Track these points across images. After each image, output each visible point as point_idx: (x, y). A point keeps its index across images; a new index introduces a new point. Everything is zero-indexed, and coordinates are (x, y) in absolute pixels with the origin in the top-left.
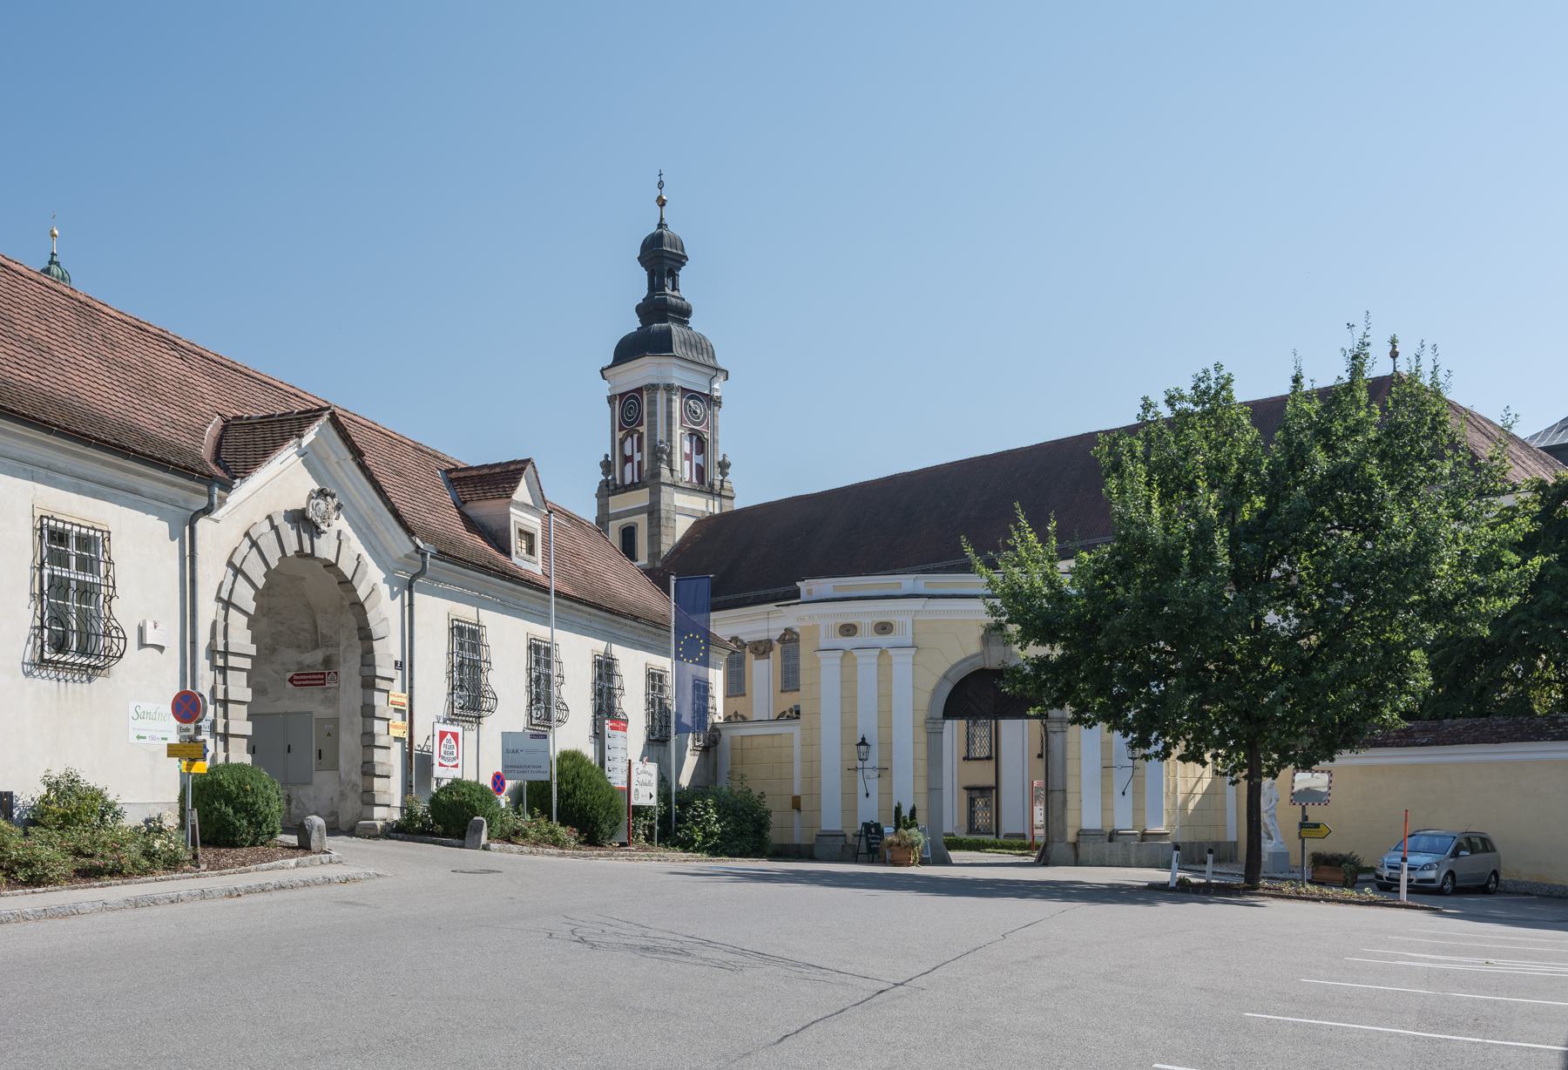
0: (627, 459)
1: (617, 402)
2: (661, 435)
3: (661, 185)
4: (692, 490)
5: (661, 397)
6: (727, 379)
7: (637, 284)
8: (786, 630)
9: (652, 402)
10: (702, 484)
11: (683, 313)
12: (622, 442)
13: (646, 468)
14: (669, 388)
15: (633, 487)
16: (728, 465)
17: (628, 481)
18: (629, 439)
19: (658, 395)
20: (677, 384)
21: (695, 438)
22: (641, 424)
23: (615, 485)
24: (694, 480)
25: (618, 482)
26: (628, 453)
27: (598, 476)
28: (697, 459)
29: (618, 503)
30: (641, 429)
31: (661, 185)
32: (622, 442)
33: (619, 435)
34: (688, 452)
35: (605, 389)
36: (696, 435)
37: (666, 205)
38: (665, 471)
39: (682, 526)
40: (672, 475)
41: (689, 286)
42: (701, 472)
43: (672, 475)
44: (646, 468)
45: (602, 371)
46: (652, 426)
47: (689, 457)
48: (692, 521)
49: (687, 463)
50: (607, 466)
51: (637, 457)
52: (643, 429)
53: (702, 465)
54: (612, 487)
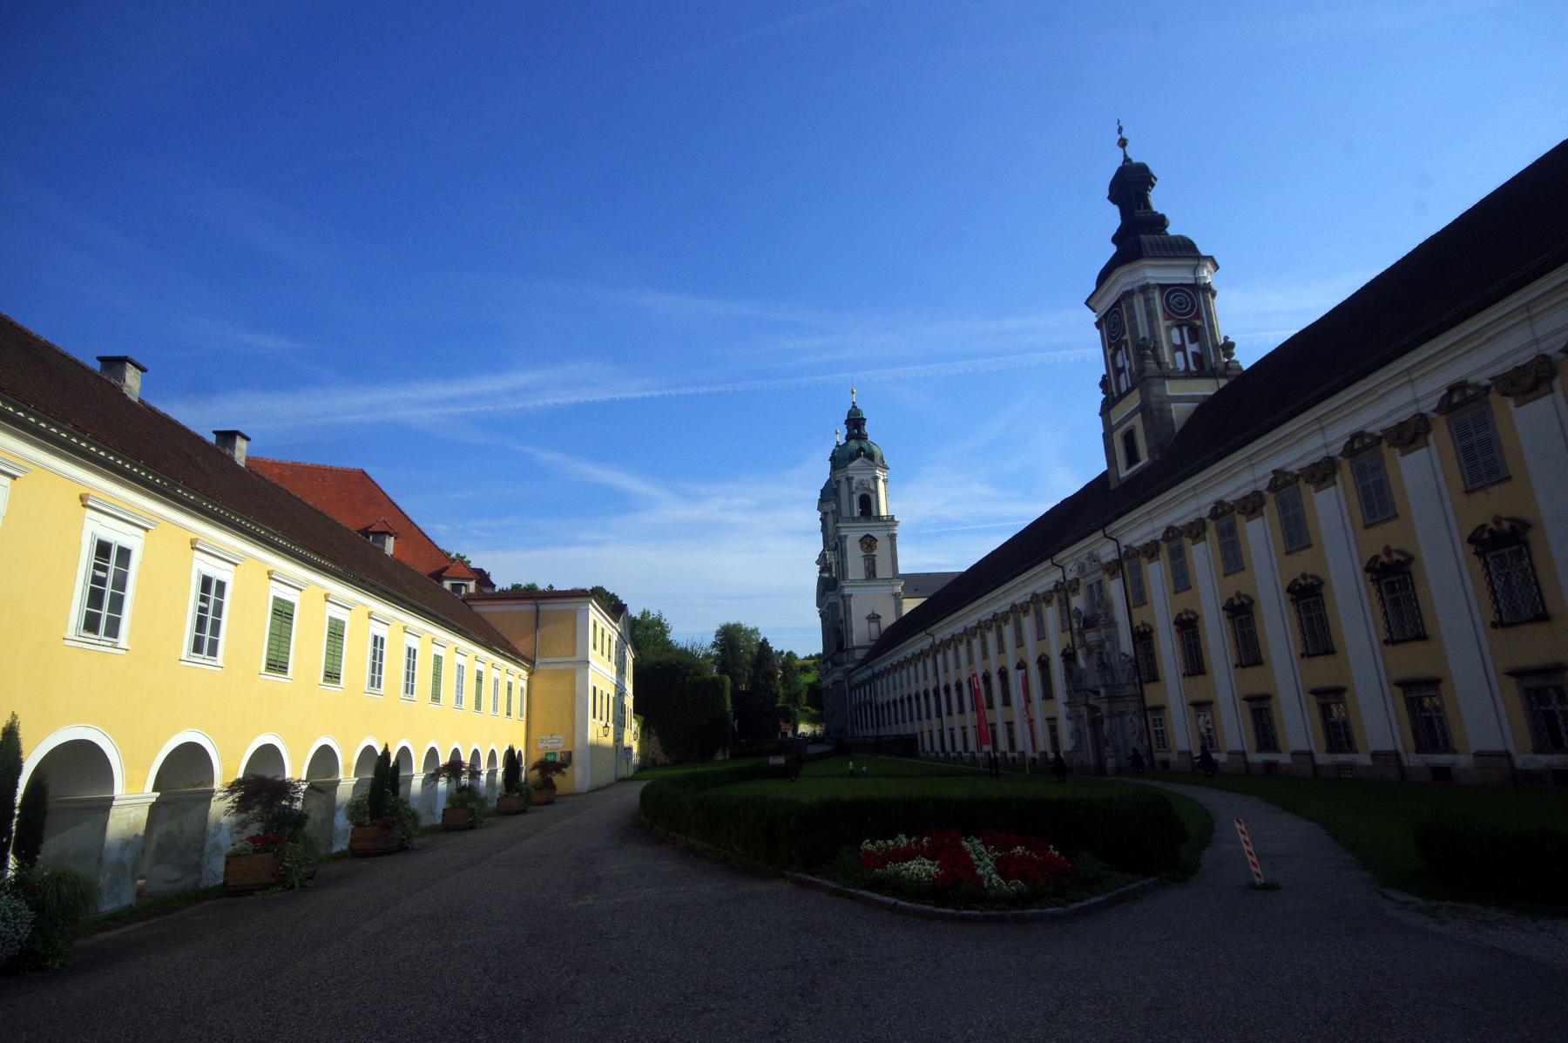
0: (1119, 371)
1: (1104, 325)
2: (1143, 331)
3: (1120, 130)
4: (1188, 375)
5: (1138, 302)
6: (1216, 267)
7: (1112, 218)
8: (1274, 472)
9: (1131, 308)
10: (1202, 368)
11: (1160, 222)
12: (1114, 357)
13: (1134, 370)
14: (1145, 289)
15: (1129, 391)
16: (1232, 345)
17: (1124, 389)
18: (1120, 352)
19: (1135, 300)
20: (1153, 282)
21: (1185, 330)
22: (1124, 333)
23: (1113, 398)
24: (1192, 368)
25: (1115, 395)
26: (1120, 364)
27: (1100, 396)
28: (1192, 348)
29: (1117, 414)
30: (1125, 338)
31: (1120, 130)
32: (1114, 357)
33: (1110, 352)
34: (1177, 341)
35: (1092, 318)
36: (1186, 325)
37: (1129, 144)
38: (1151, 364)
39: (1180, 413)
40: (1160, 368)
41: (1158, 200)
42: (1198, 358)
43: (1160, 368)
44: (1134, 370)
45: (1087, 303)
46: (1134, 328)
47: (1182, 348)
48: (1193, 406)
49: (1179, 355)
50: (1104, 384)
51: (1127, 366)
52: (1127, 337)
53: (1199, 352)
54: (1110, 402)
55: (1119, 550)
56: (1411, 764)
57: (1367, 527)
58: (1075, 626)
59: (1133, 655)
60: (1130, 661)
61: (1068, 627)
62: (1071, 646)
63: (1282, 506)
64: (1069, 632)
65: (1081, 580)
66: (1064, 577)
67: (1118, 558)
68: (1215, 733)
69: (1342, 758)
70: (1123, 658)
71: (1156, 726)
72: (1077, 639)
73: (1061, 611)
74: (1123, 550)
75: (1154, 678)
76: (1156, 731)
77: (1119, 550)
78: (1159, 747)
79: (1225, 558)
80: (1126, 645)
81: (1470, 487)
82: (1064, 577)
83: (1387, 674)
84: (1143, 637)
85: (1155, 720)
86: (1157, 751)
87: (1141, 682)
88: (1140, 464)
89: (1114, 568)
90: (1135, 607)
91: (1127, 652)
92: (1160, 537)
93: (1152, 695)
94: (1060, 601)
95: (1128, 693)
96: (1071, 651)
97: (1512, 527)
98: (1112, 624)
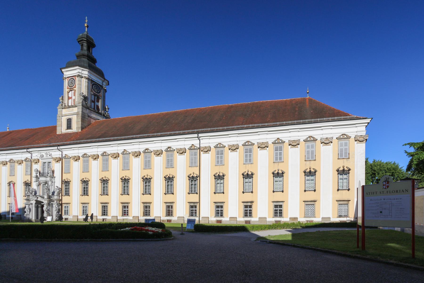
8: (124, 150)
23: (65, 105)
55: (62, 155)
56: (141, 219)
57: (144, 169)
58: (34, 174)
59: (60, 187)
60: (59, 189)
61: (29, 173)
62: (30, 180)
63: (124, 159)
64: (30, 176)
65: (40, 160)
66: (31, 157)
67: (61, 157)
68: (88, 211)
69: (125, 217)
70: (56, 188)
71: (65, 208)
72: (34, 179)
73: (26, 168)
74: (63, 156)
75: (67, 194)
76: (65, 210)
77: (62, 155)
78: (65, 214)
79: (103, 167)
80: (58, 183)
81: (167, 167)
82: (31, 157)
83: (141, 200)
84: (67, 183)
85: (65, 207)
86: (64, 215)
87: (62, 195)
88: (72, 130)
89: (59, 160)
90: (64, 173)
91: (58, 186)
92: (81, 155)
93: (65, 199)
94: (27, 165)
95: (56, 198)
96: (29, 182)
97: (172, 177)
98: (53, 177)
